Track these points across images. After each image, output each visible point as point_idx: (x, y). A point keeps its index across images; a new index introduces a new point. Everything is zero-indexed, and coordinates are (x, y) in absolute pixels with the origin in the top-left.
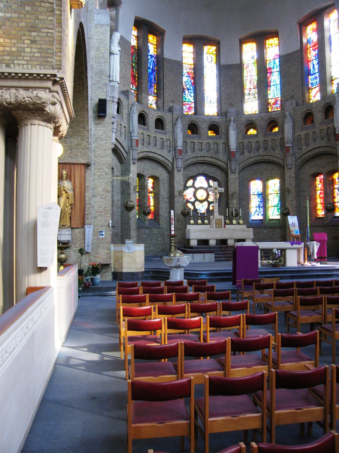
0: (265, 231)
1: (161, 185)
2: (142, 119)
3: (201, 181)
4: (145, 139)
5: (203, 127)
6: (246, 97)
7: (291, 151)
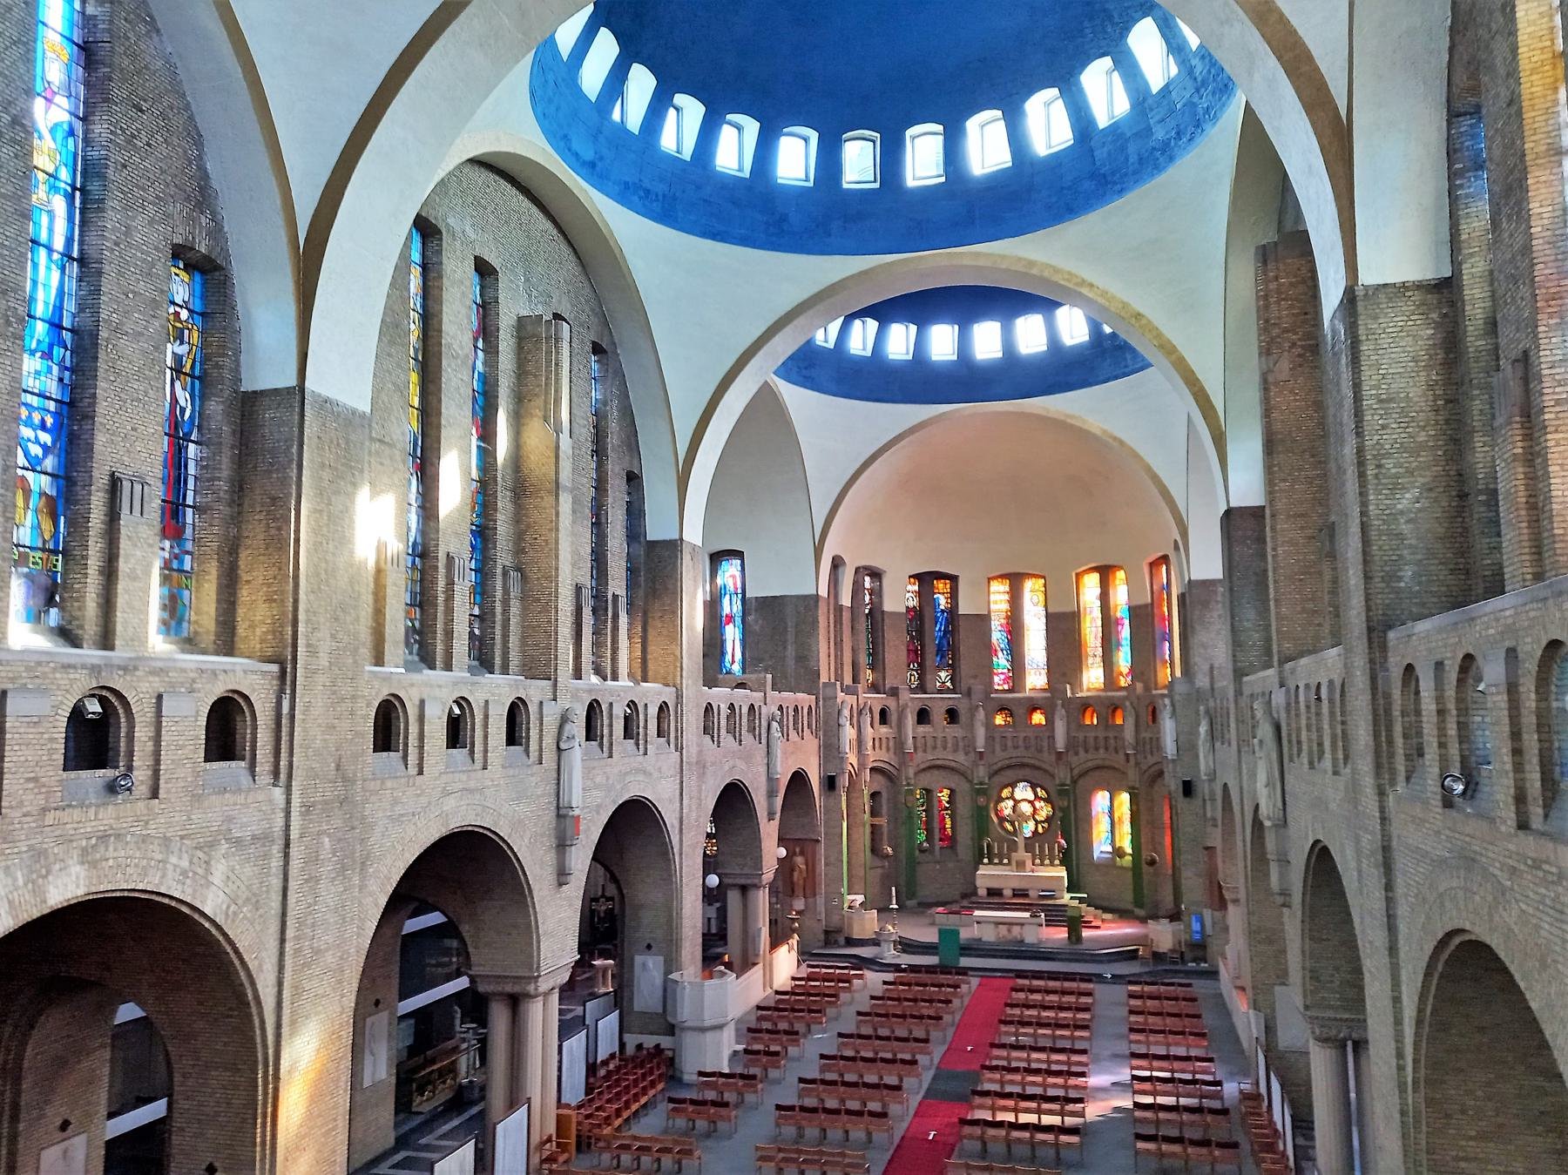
1: (959, 798)
2: (923, 716)
3: (1023, 792)
6: (1090, 660)
7: (1132, 759)
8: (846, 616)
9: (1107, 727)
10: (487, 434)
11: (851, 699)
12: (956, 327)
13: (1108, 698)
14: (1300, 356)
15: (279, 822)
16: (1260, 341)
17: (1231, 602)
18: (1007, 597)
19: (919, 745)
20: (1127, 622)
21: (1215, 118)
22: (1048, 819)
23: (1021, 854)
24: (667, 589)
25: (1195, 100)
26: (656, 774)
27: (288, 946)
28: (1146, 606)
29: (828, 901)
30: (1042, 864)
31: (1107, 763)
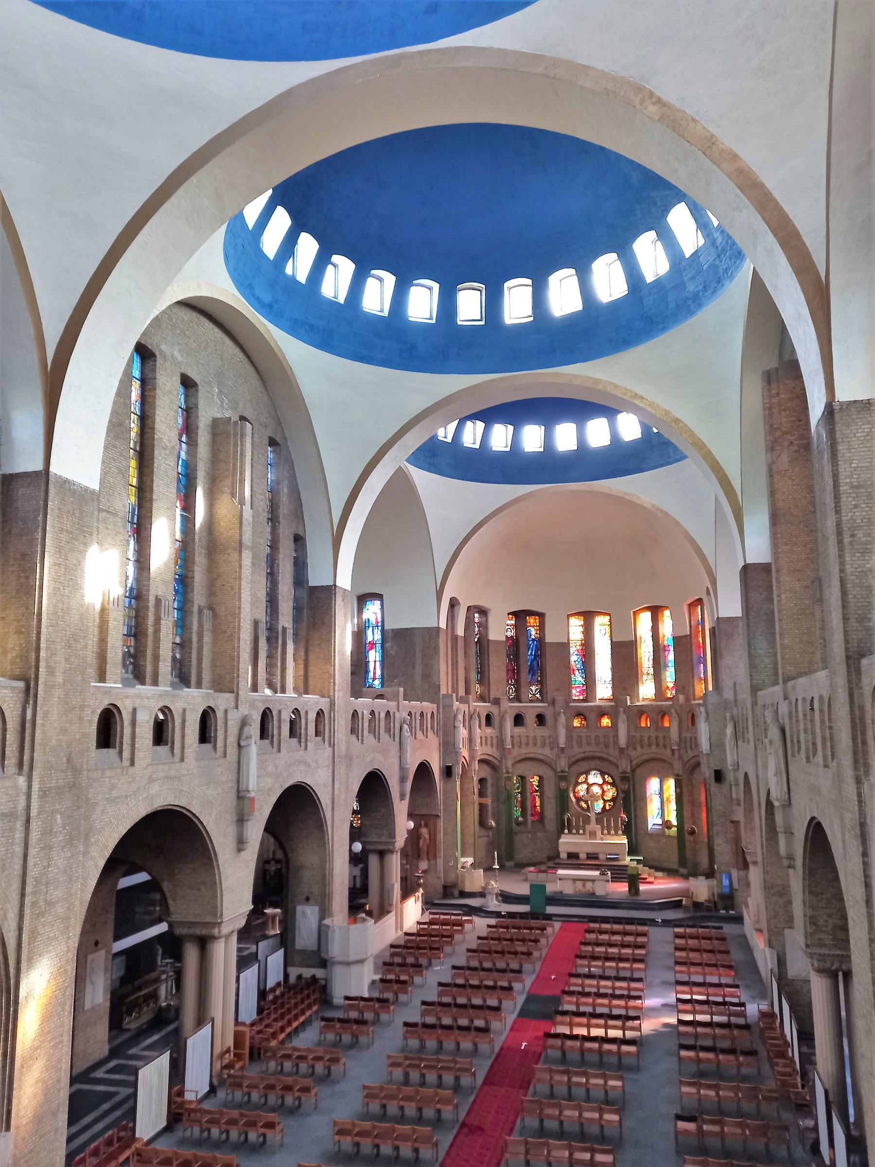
0: (665, 840)
1: (546, 784)
2: (519, 720)
3: (595, 778)
4: (522, 741)
5: (592, 716)
6: (645, 677)
7: (677, 754)
8: (461, 643)
9: (658, 729)
10: (188, 506)
11: (464, 707)
12: (543, 428)
13: (658, 706)
14: (795, 451)
15: (22, 803)
16: (766, 441)
17: (748, 635)
18: (581, 629)
19: (515, 742)
20: (671, 648)
21: (731, 277)
22: (613, 799)
23: (593, 826)
24: (324, 623)
25: (717, 262)
26: (314, 765)
27: (28, 900)
28: (686, 636)
29: (446, 862)
30: (609, 833)
31: (658, 756)
